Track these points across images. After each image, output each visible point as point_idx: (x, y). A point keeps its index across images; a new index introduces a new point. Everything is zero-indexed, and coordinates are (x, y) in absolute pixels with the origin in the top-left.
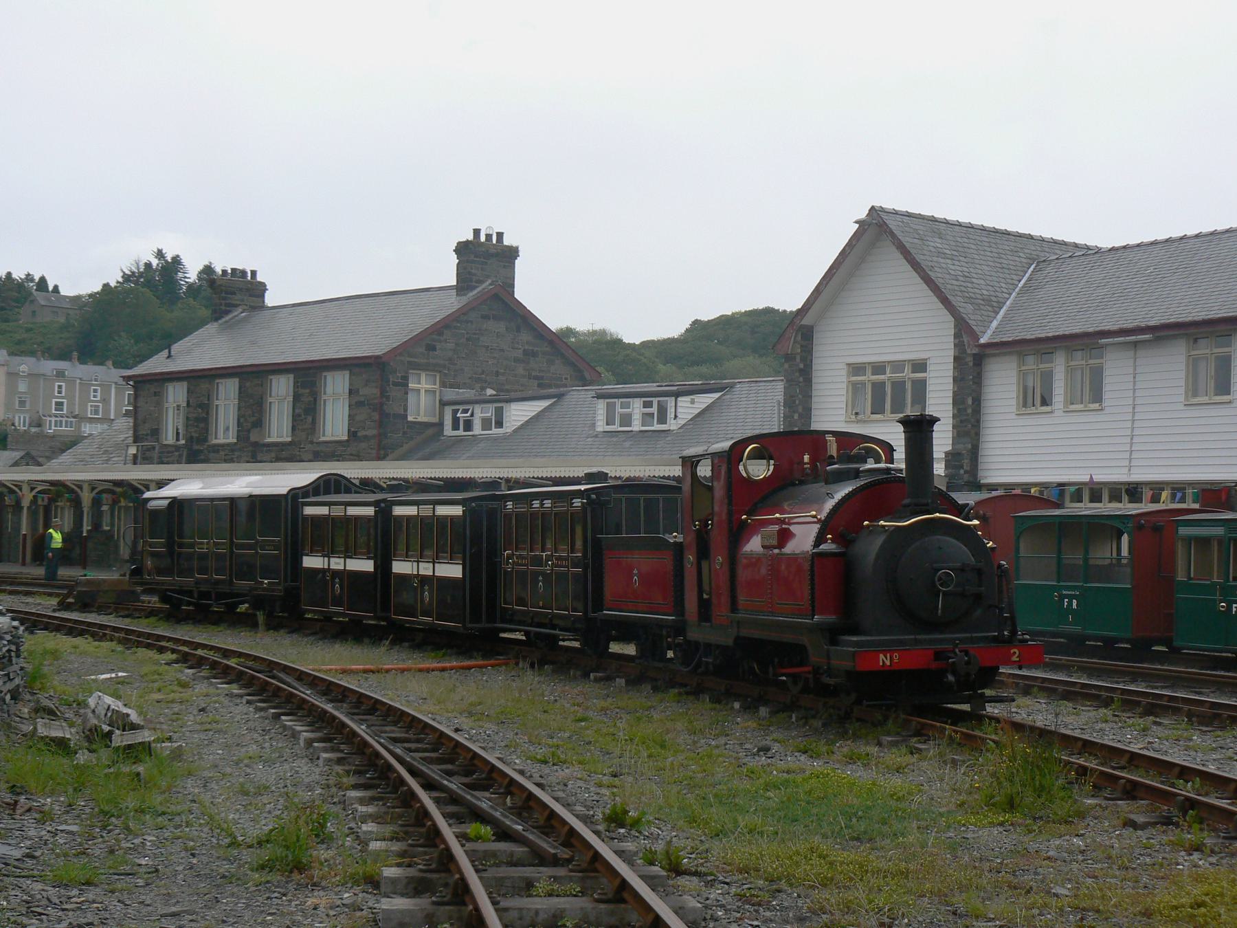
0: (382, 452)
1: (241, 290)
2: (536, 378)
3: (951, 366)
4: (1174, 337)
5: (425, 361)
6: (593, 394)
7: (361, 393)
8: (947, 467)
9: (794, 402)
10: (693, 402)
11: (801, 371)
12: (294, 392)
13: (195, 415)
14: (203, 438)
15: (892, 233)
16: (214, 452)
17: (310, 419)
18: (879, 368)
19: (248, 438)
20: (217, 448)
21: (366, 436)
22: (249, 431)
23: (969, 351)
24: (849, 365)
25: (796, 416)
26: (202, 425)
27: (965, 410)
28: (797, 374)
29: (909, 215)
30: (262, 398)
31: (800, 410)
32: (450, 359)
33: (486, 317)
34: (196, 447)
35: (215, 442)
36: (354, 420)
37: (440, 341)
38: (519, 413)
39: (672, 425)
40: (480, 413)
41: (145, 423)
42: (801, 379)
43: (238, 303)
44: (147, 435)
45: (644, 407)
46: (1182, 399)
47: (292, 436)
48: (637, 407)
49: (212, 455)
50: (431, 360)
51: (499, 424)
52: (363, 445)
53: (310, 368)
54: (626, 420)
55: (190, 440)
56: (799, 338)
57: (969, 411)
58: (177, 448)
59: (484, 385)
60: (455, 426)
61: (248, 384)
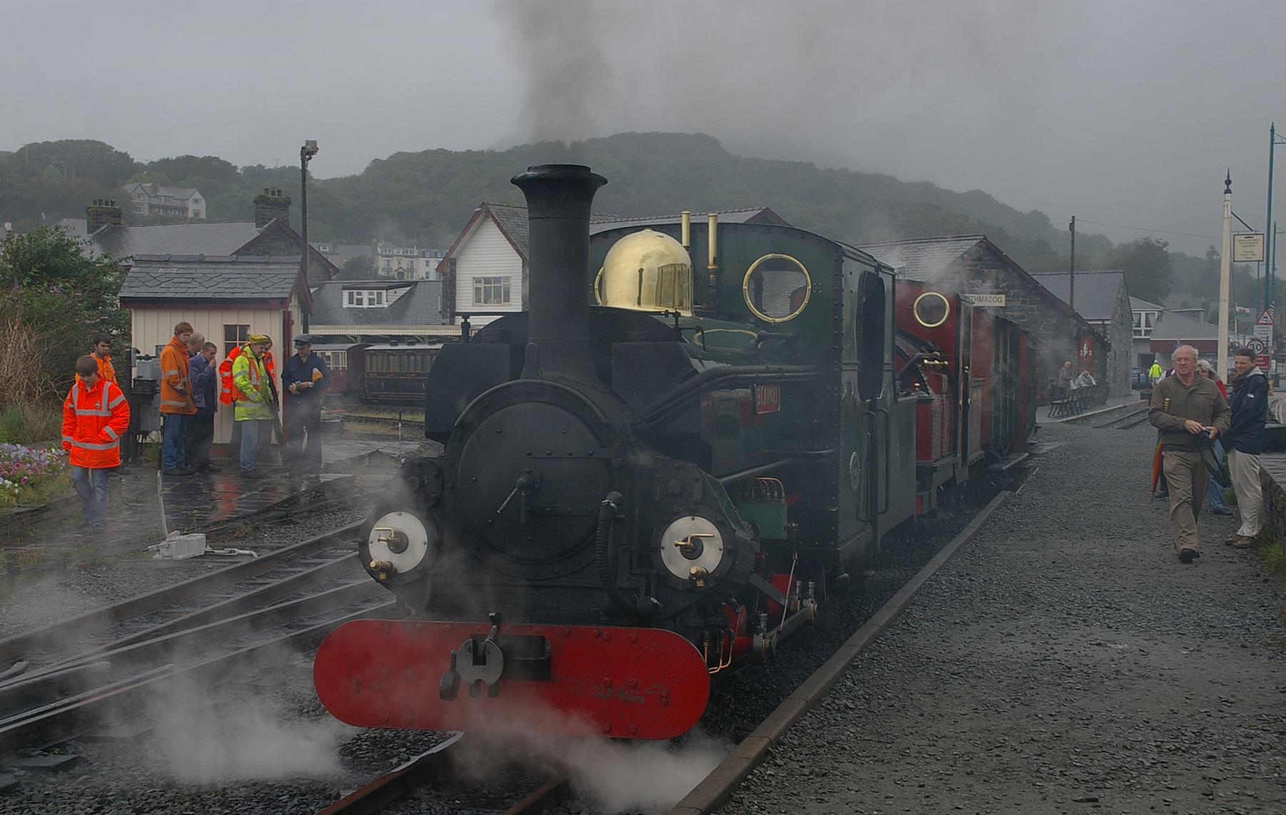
10: (395, 292)
15: (493, 217)
18: (487, 280)
24: (474, 278)
33: (274, 240)
39: (385, 305)
48: (365, 295)
54: (360, 302)
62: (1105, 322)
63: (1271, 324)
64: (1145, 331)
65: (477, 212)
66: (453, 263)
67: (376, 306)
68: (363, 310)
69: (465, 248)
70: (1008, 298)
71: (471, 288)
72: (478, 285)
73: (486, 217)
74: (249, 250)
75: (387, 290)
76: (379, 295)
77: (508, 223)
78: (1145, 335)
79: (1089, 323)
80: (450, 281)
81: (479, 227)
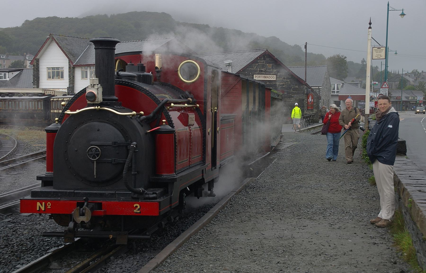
8: (68, 90)
15: (55, 40)
18: (53, 68)
24: (47, 67)
62: (320, 88)
63: (387, 88)
64: (337, 91)
65: (48, 38)
66: (38, 61)
69: (43, 54)
70: (277, 77)
71: (46, 72)
72: (49, 71)
73: (52, 40)
77: (62, 43)
78: (337, 93)
79: (312, 88)
80: (36, 69)
81: (49, 45)
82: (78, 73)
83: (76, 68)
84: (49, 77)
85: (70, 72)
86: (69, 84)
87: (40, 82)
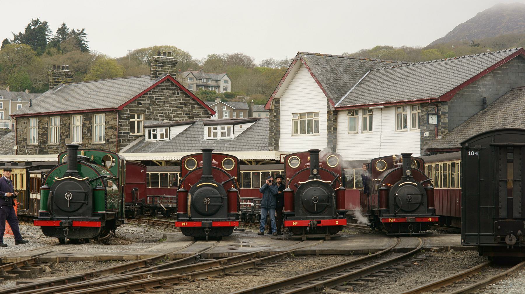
0: (119, 148)
1: (61, 75)
2: (186, 114)
3: (326, 115)
4: (392, 106)
5: (137, 109)
6: (203, 124)
7: (110, 123)
9: (272, 129)
10: (241, 127)
11: (275, 116)
12: (83, 123)
13: (42, 132)
14: (45, 142)
16: (50, 148)
17: (89, 134)
19: (64, 142)
20: (51, 147)
21: (112, 142)
22: (64, 139)
23: (331, 110)
25: (273, 134)
26: (45, 137)
27: (331, 132)
28: (273, 117)
29: (314, 54)
30: (70, 125)
31: (275, 131)
32: (148, 108)
33: (164, 89)
34: (42, 146)
35: (50, 144)
36: (107, 135)
37: (143, 100)
38: (175, 131)
40: (159, 131)
41: (20, 135)
42: (275, 119)
43: (60, 81)
44: (22, 141)
45: (222, 129)
46: (394, 129)
47: (83, 141)
49: (49, 150)
50: (139, 108)
51: (167, 136)
52: (111, 145)
53: (89, 112)
54: (216, 135)
55: (40, 143)
56: (274, 103)
57: (332, 133)
58: (35, 146)
59: (163, 118)
60: (150, 137)
61: (64, 119)
66: (277, 102)
67: (227, 137)
68: (217, 142)
69: (286, 89)
74: (143, 97)
75: (234, 125)
76: (229, 129)
82: (344, 120)
83: (340, 113)
84: (296, 131)
85: (330, 120)
86: (327, 143)
87: (280, 140)
